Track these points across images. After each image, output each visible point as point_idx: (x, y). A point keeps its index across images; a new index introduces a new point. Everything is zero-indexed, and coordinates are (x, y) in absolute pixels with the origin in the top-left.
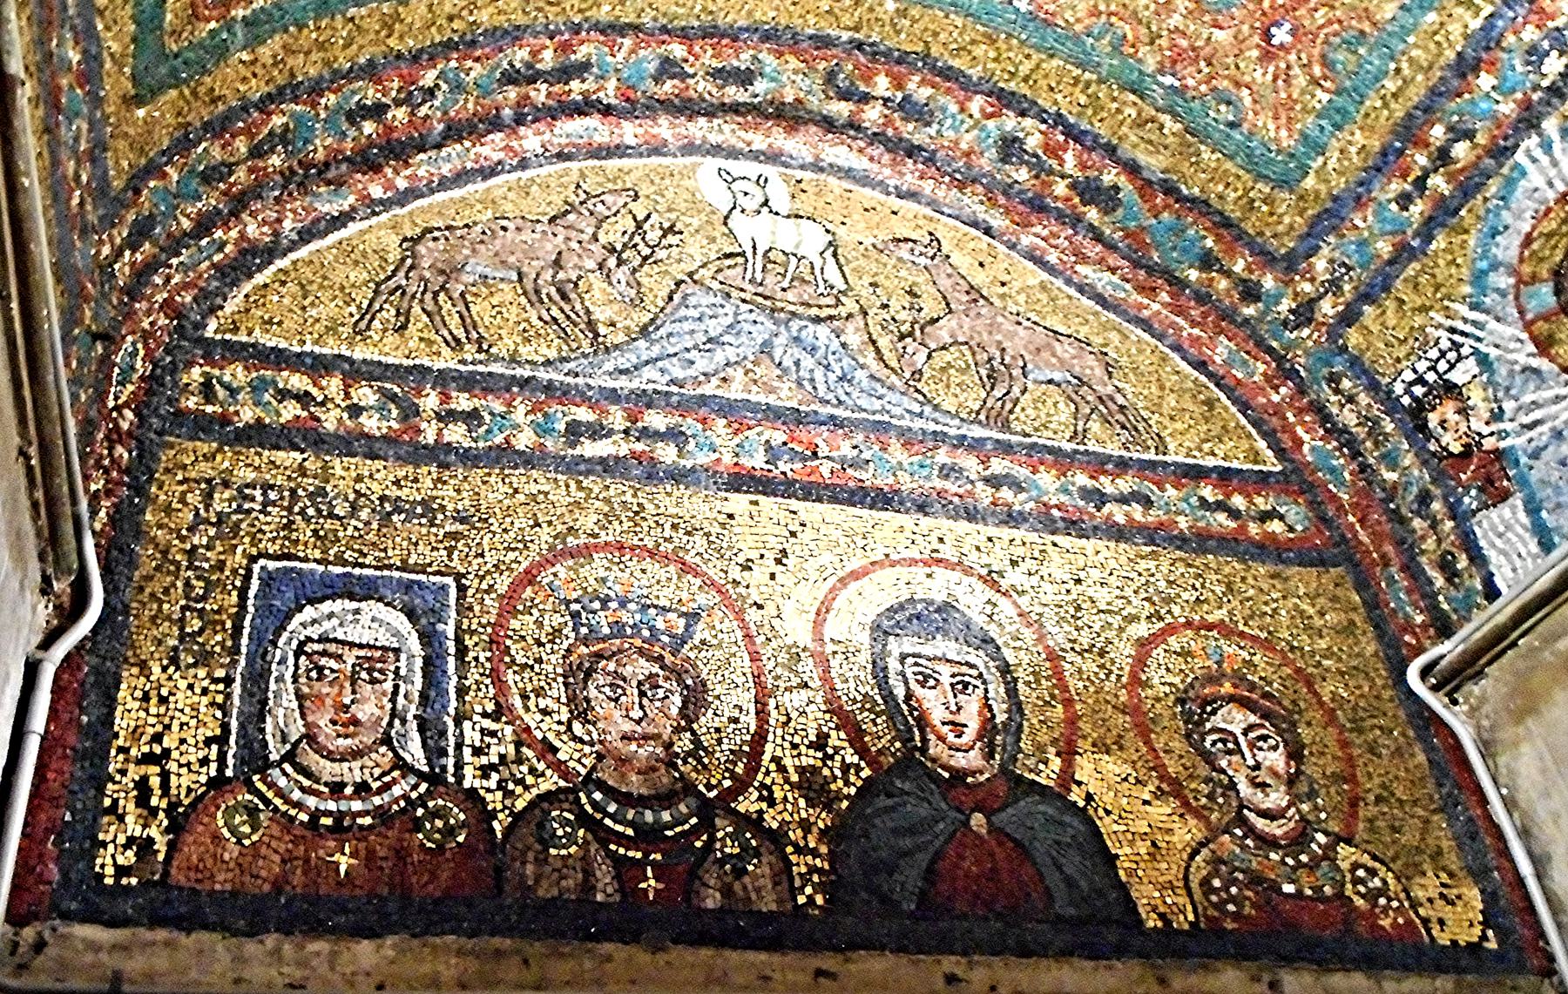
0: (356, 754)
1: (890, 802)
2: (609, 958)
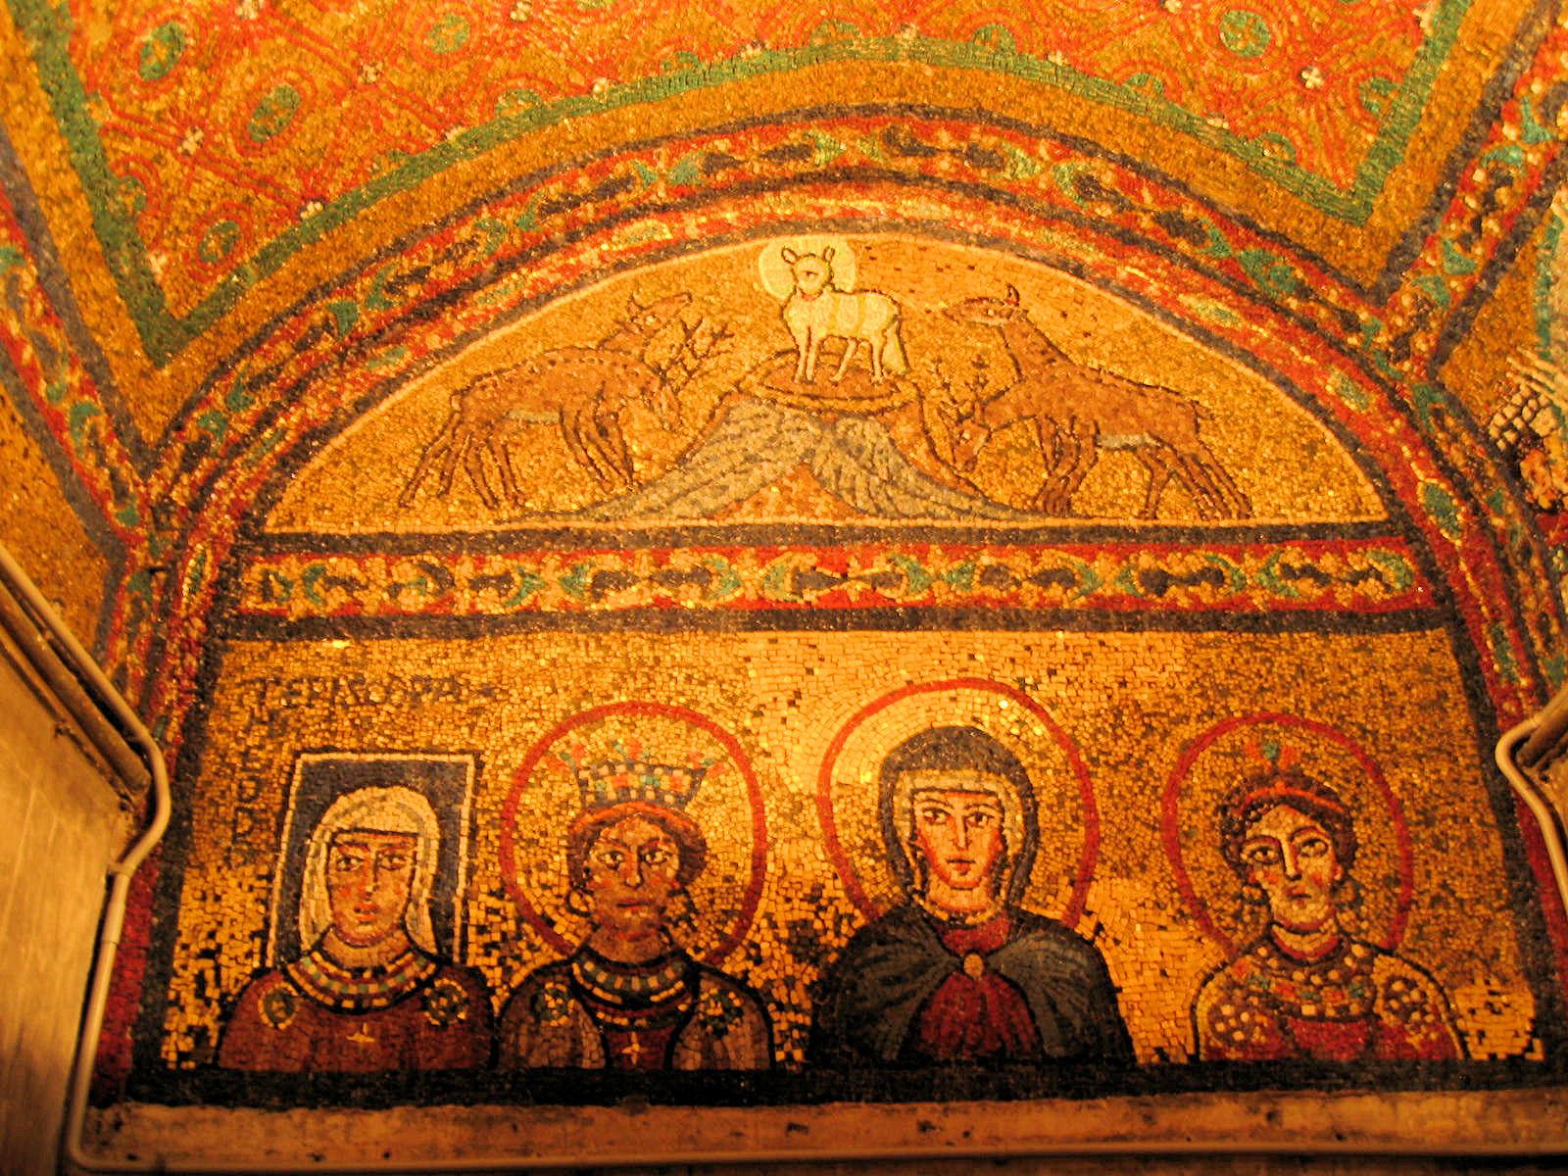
0: (375, 940)
1: (881, 950)
2: (590, 1121)
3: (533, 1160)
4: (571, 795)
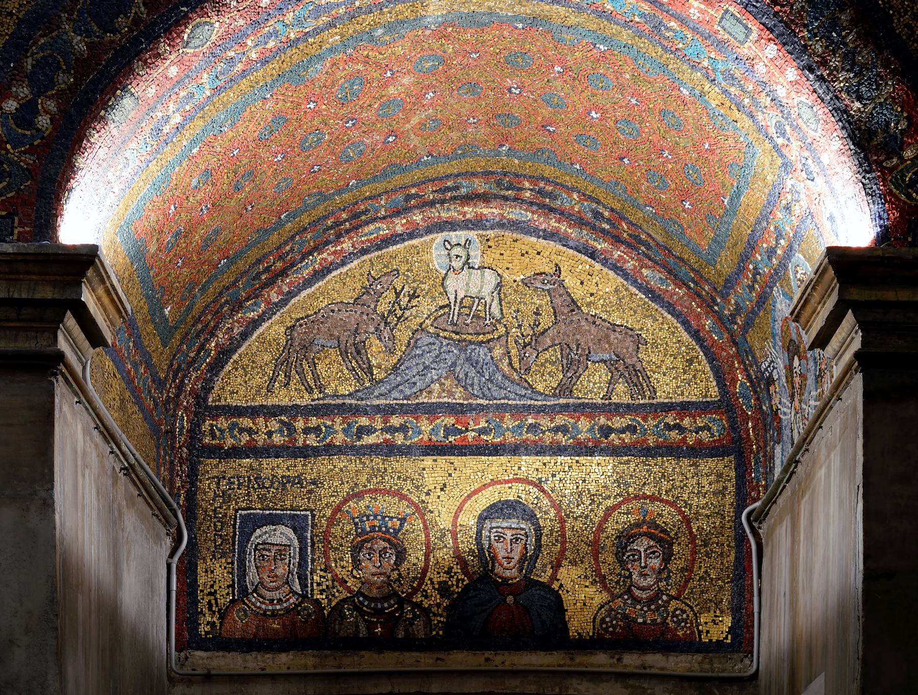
0: (277, 588)
1: (474, 594)
2: (363, 656)
3: (342, 670)
4: (351, 529)
